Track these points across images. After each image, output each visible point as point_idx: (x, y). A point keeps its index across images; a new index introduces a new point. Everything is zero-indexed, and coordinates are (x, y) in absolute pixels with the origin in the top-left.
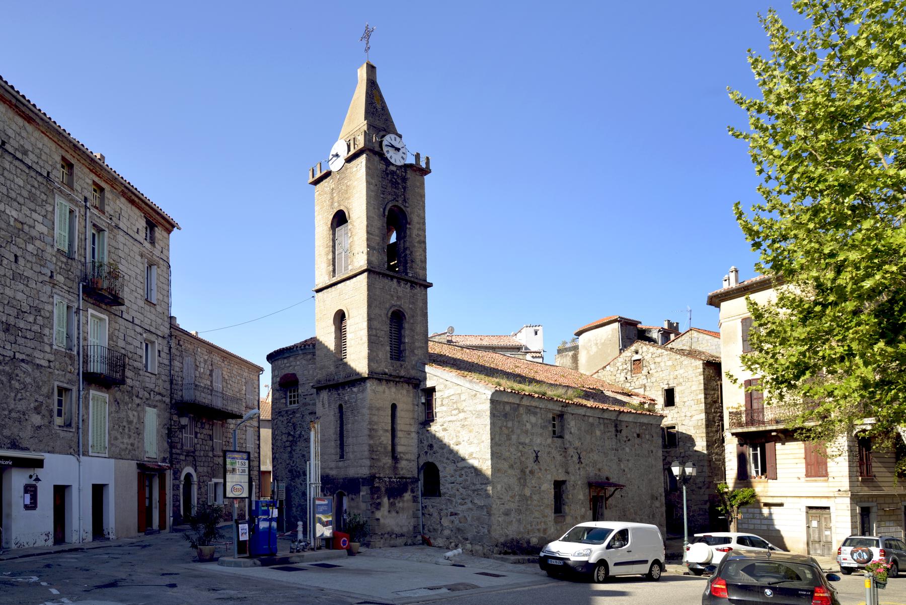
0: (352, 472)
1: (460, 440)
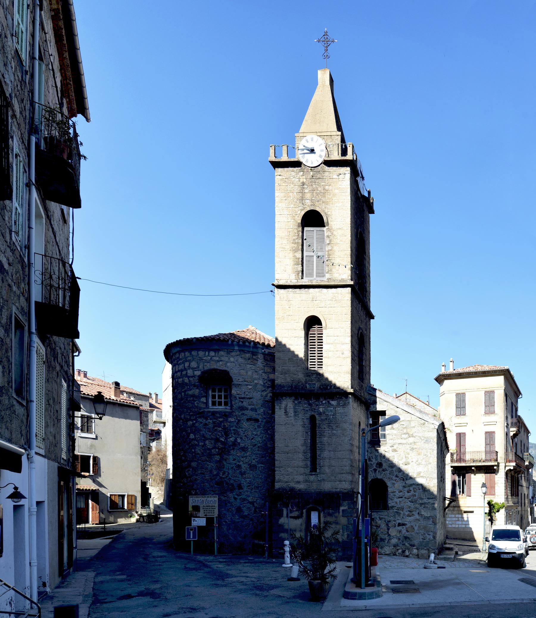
0: (327, 486)
1: (409, 460)
